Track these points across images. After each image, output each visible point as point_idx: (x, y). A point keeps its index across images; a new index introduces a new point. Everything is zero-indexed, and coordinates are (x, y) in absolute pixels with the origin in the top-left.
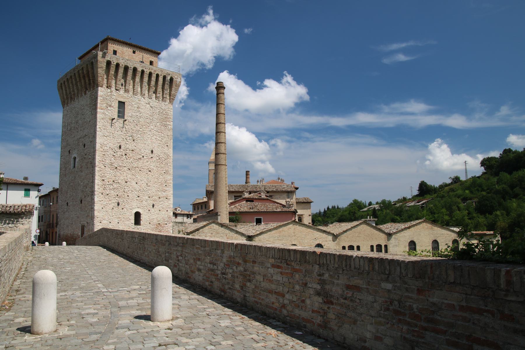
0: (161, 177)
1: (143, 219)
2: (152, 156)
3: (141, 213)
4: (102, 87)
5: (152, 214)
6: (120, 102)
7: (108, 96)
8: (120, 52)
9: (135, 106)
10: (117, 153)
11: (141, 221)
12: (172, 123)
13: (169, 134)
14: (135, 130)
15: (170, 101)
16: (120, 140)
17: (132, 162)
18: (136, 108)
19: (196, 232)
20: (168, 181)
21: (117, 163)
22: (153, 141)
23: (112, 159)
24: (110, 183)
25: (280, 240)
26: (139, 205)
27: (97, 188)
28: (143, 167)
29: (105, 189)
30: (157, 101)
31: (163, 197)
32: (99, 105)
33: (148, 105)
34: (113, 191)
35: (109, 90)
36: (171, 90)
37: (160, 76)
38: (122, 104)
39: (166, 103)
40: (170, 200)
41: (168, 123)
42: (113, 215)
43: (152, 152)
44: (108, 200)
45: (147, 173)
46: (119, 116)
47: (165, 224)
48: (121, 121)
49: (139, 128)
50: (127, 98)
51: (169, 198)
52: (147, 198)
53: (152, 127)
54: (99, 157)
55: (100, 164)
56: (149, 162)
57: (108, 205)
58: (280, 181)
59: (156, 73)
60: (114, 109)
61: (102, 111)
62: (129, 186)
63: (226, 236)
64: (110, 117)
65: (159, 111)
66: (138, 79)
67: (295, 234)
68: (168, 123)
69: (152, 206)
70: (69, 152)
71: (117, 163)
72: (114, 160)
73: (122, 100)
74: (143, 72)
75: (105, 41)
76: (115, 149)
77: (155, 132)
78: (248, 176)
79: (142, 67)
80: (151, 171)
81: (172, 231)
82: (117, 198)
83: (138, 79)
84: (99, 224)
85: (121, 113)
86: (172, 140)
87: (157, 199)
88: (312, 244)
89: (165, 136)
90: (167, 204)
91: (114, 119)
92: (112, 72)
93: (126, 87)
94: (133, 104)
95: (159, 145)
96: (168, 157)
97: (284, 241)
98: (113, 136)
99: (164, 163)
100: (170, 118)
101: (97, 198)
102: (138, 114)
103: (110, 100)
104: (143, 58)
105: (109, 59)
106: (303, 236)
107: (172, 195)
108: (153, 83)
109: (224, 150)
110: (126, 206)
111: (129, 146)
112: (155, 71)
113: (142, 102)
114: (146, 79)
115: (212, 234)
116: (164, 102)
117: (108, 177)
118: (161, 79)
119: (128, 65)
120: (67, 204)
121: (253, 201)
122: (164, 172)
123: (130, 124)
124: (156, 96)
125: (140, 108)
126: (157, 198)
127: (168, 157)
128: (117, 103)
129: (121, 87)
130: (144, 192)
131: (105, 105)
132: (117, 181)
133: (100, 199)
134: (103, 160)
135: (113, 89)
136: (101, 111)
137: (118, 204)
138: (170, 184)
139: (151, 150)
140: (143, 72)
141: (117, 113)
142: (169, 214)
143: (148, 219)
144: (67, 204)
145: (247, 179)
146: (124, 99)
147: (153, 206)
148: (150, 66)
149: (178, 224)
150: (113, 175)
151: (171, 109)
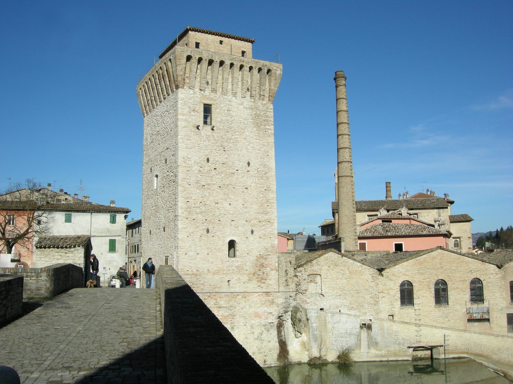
0: (262, 196)
1: (239, 250)
2: (249, 169)
3: (237, 242)
4: (183, 88)
5: (251, 242)
6: (205, 105)
7: (191, 99)
8: (204, 44)
9: (225, 108)
10: (205, 168)
11: (237, 252)
12: (273, 126)
13: (270, 141)
14: (226, 138)
15: (269, 99)
16: (207, 152)
17: (224, 178)
18: (226, 112)
19: (309, 265)
20: (270, 201)
21: (204, 180)
22: (249, 150)
23: (199, 175)
24: (197, 205)
26: (234, 232)
27: (180, 213)
28: (237, 184)
29: (190, 212)
30: (252, 100)
31: (265, 221)
32: (180, 111)
33: (241, 106)
34: (200, 215)
35: (192, 92)
37: (254, 68)
39: (264, 102)
40: (273, 224)
41: (267, 127)
42: (202, 244)
43: (249, 164)
44: (194, 226)
45: (243, 192)
46: (205, 123)
47: (267, 256)
48: (209, 128)
49: (231, 136)
50: (215, 100)
51: (272, 221)
52: (244, 222)
53: (248, 133)
54: (182, 175)
55: (184, 182)
56: (245, 178)
57: (195, 233)
58: (429, 193)
59: (249, 66)
60: (198, 114)
61: (184, 117)
62: (221, 209)
63: (348, 269)
64: (193, 124)
65: (255, 112)
67: (442, 265)
68: (267, 127)
69: (250, 233)
70: (151, 169)
71: (204, 180)
72: (201, 177)
73: (208, 102)
75: (186, 32)
76: (202, 163)
77: (251, 139)
78: (388, 188)
79: (231, 60)
80: (249, 188)
81: (277, 264)
82: (205, 224)
84: (184, 256)
86: (273, 149)
87: (256, 223)
88: (466, 278)
89: (265, 143)
90: (270, 229)
91: (199, 126)
93: (213, 86)
94: (222, 106)
95: (257, 155)
96: (270, 170)
97: (426, 275)
98: (199, 147)
99: (264, 178)
100: (271, 121)
101: (182, 224)
102: (228, 118)
103: (193, 103)
104: (231, 48)
105: (190, 54)
106: (453, 268)
107: (276, 218)
109: (349, 157)
110: (218, 233)
111: (219, 158)
112: (248, 63)
113: (233, 104)
115: (329, 267)
116: (261, 101)
117: (193, 198)
119: (214, 59)
120: (150, 232)
121: (391, 222)
122: (265, 189)
123: (219, 131)
124: (251, 94)
125: (231, 110)
126: (256, 222)
127: (270, 170)
128: (202, 107)
129: (206, 86)
130: (240, 216)
131: (188, 109)
132: (205, 203)
133: (185, 226)
134: (187, 177)
135: (197, 90)
136: (183, 117)
137: (208, 231)
138: (273, 204)
139: (247, 162)
141: (203, 118)
142: (273, 242)
143: (246, 250)
144: (150, 232)
145: (388, 192)
146: (211, 100)
147: (252, 232)
148: (242, 58)
149: (285, 255)
150: (200, 196)
151: (271, 109)
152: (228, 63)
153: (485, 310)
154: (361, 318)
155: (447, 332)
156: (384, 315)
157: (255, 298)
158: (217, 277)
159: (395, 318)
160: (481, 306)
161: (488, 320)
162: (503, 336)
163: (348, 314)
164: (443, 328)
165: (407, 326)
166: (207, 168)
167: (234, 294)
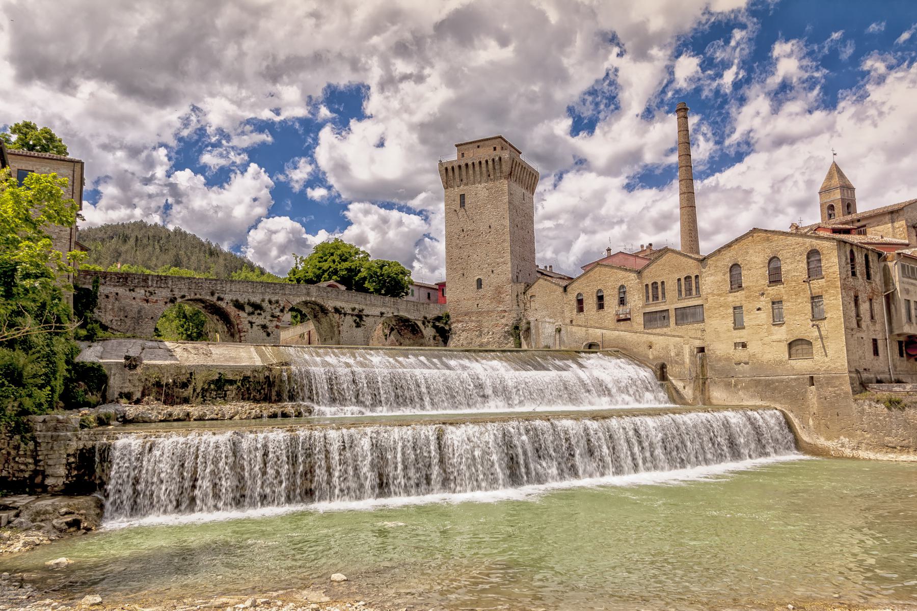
25: (588, 286)
36: (501, 168)
38: (462, 197)
66: (471, 172)
74: (473, 164)
83: (471, 172)
85: (462, 204)
92: (450, 173)
108: (484, 169)
114: (477, 168)
118: (490, 163)
140: (473, 164)
152: (470, 163)
153: (628, 311)
154: (556, 324)
155: (604, 331)
156: (568, 321)
157: (494, 315)
158: (470, 302)
159: (574, 323)
160: (625, 307)
161: (629, 319)
162: (640, 333)
163: (549, 322)
164: (600, 328)
165: (580, 328)
166: (463, 235)
167: (480, 313)
